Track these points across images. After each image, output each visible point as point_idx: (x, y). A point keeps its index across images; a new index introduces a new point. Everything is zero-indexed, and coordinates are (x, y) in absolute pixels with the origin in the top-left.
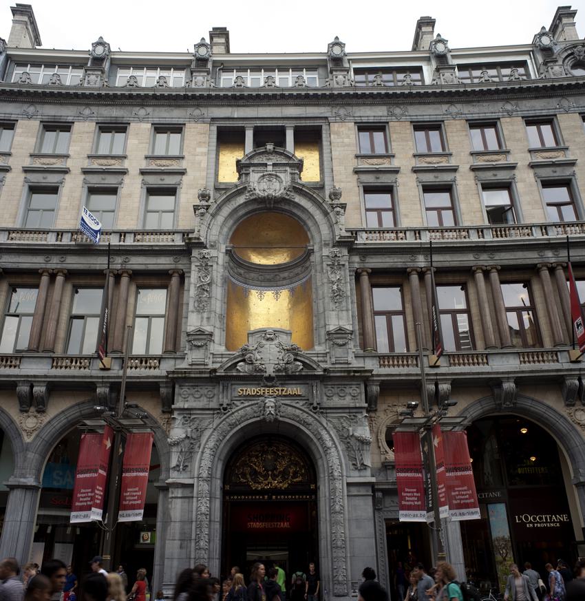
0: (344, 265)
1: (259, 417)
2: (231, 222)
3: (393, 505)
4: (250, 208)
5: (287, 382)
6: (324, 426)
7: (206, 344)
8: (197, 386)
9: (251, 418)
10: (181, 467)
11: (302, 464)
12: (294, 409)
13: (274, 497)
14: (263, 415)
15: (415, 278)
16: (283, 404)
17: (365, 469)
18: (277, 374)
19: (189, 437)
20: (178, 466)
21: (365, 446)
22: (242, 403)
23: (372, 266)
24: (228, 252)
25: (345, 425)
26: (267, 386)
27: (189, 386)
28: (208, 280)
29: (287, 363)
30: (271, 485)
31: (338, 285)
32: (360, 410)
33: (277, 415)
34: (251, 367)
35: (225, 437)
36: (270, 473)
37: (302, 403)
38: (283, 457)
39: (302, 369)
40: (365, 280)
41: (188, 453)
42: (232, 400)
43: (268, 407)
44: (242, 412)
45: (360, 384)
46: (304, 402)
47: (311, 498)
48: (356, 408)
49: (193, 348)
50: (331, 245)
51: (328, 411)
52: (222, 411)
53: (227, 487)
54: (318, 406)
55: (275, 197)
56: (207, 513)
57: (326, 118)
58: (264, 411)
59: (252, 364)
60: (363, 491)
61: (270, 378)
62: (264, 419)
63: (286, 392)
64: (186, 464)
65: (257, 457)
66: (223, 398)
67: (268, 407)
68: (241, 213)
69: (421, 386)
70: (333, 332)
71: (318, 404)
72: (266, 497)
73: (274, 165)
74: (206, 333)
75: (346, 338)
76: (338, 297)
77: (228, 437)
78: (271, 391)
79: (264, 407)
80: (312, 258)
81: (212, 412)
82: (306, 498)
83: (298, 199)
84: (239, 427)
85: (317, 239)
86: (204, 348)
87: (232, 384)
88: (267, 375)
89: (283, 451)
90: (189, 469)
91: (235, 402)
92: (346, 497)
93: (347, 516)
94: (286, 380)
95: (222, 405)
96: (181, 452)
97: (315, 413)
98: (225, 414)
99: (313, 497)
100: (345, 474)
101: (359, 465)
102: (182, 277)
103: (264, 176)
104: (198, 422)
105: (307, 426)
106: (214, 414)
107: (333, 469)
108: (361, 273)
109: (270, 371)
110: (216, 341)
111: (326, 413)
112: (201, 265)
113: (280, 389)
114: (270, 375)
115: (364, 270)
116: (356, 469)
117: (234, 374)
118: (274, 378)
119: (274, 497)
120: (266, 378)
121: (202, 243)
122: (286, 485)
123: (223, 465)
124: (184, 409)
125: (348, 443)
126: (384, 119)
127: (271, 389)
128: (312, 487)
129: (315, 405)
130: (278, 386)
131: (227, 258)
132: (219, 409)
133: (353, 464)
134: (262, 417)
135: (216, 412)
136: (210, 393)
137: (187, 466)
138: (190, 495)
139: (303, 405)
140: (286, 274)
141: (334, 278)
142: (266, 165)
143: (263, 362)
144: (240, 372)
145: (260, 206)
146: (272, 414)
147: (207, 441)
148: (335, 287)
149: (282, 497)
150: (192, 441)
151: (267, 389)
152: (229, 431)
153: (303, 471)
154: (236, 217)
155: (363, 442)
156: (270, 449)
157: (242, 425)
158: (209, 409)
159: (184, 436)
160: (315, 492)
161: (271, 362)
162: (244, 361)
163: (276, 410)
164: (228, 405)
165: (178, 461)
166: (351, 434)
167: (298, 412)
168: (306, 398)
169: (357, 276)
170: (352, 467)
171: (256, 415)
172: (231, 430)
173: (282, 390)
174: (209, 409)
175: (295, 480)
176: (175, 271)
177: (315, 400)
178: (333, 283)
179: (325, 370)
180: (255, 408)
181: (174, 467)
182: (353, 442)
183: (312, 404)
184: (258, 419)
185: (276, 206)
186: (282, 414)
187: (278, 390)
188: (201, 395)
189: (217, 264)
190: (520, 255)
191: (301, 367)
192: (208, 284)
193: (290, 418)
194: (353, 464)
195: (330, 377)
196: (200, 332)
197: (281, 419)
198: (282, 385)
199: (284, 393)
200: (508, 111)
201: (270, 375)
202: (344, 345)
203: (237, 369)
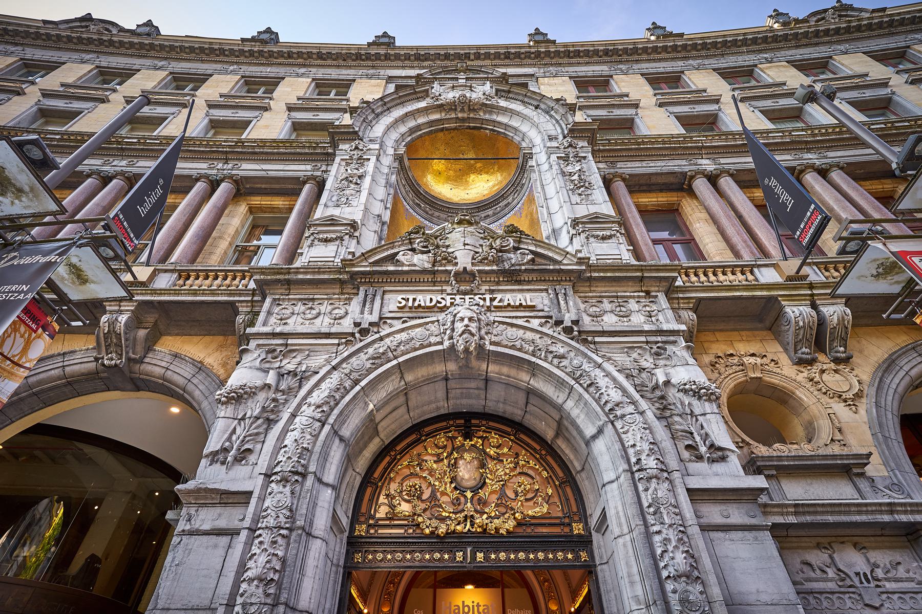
0: (585, 158)
1: (441, 343)
2: (403, 129)
3: (813, 575)
4: (436, 116)
5: (501, 288)
6: (595, 362)
7: (342, 239)
8: (313, 300)
9: (422, 347)
10: (233, 452)
11: (545, 474)
12: (522, 331)
13: (480, 556)
14: (451, 338)
15: (701, 186)
16: (495, 322)
17: (723, 459)
18: (481, 268)
19: (269, 386)
20: (225, 450)
21: (707, 404)
22: (404, 322)
23: (629, 171)
24: (399, 158)
25: (645, 364)
26: (459, 292)
27: (294, 299)
28: (359, 173)
29: (501, 251)
30: (472, 525)
31: (579, 176)
32: (672, 338)
33: (481, 338)
34: (425, 257)
35: (356, 382)
36: (469, 494)
37: (535, 323)
38: (498, 459)
39: (533, 260)
40: (620, 187)
41: (260, 421)
42: (381, 318)
43: (462, 319)
44: (403, 336)
45: (656, 297)
46: (543, 320)
47: (577, 558)
48: (660, 332)
49: (316, 242)
50: (561, 137)
51: (597, 339)
52: (357, 335)
53: (361, 530)
54: (576, 329)
55: (470, 101)
56: (271, 575)
57: (532, 75)
58: (453, 330)
59: (429, 252)
60: (737, 515)
61: (465, 276)
62: (452, 347)
63: (501, 301)
64: (246, 446)
65: (439, 460)
66: (362, 313)
67: (462, 319)
68: (421, 120)
69: (781, 312)
70: (584, 220)
71: (576, 322)
72: (459, 555)
73: (467, 79)
74: (345, 222)
75: (610, 229)
76: (582, 189)
77: (363, 383)
78: (467, 300)
79: (453, 322)
80: (532, 163)
81: (336, 341)
82: (566, 559)
83: (503, 103)
84: (395, 362)
85: (538, 140)
86: (337, 243)
87: (384, 292)
88: (460, 267)
89: (497, 447)
90: (252, 458)
91: (389, 321)
92: (696, 529)
93: (716, 592)
94: (498, 283)
95: (357, 324)
96: (243, 419)
97: (572, 339)
98: (361, 341)
99: (584, 555)
100: (673, 463)
101: (703, 449)
102: (321, 185)
103: (453, 87)
104: (298, 359)
105: (556, 361)
106: (339, 345)
107: (638, 453)
108: (611, 180)
109: (464, 260)
110: (361, 241)
111: (595, 343)
112: (351, 158)
113: (488, 297)
114: (465, 268)
115: (615, 175)
116: (700, 458)
117: (391, 268)
118: (472, 275)
119: (480, 556)
120: (457, 274)
121: (356, 133)
122: (511, 524)
123: (349, 460)
124: (274, 335)
125: (662, 397)
126: (607, 73)
127: (467, 297)
128: (578, 528)
129: (567, 323)
130: (483, 294)
131: (396, 164)
132: (353, 334)
133: (688, 447)
134: (447, 344)
135: (344, 340)
136: (336, 311)
137: (249, 451)
138: (236, 524)
139: (541, 325)
140: (490, 212)
141: (570, 169)
142: (457, 79)
143: (450, 250)
144: (403, 265)
145: (448, 116)
146: (473, 335)
147: (310, 392)
148: (576, 177)
149: (502, 555)
150: (279, 396)
151: (458, 297)
152: (370, 371)
153: (550, 491)
154: (412, 124)
155: (697, 393)
156: (468, 443)
157: (401, 359)
158: (328, 335)
159: (259, 383)
160: (585, 542)
161: (467, 247)
162: (413, 250)
163: (480, 329)
164: (371, 324)
165: (229, 439)
166: (662, 379)
167: (529, 335)
168: (546, 314)
169: (607, 183)
170: (686, 455)
171: (433, 339)
172: (376, 369)
173: (492, 300)
174: (328, 335)
175: (530, 513)
176: (313, 178)
177: (567, 315)
178: (570, 174)
179: (581, 261)
180: (433, 328)
181: (215, 454)
182: (673, 395)
183: (559, 323)
184: (440, 347)
185: (472, 115)
186: (494, 339)
187: (484, 299)
188: (319, 314)
189: (378, 160)
190: (845, 187)
191: (530, 257)
192: (360, 177)
193: (513, 347)
194: (688, 447)
195: (590, 279)
196: (332, 221)
197: (493, 348)
198: (492, 292)
199: (495, 303)
200: (766, 58)
201: (465, 268)
202: (610, 237)
203: (398, 261)
